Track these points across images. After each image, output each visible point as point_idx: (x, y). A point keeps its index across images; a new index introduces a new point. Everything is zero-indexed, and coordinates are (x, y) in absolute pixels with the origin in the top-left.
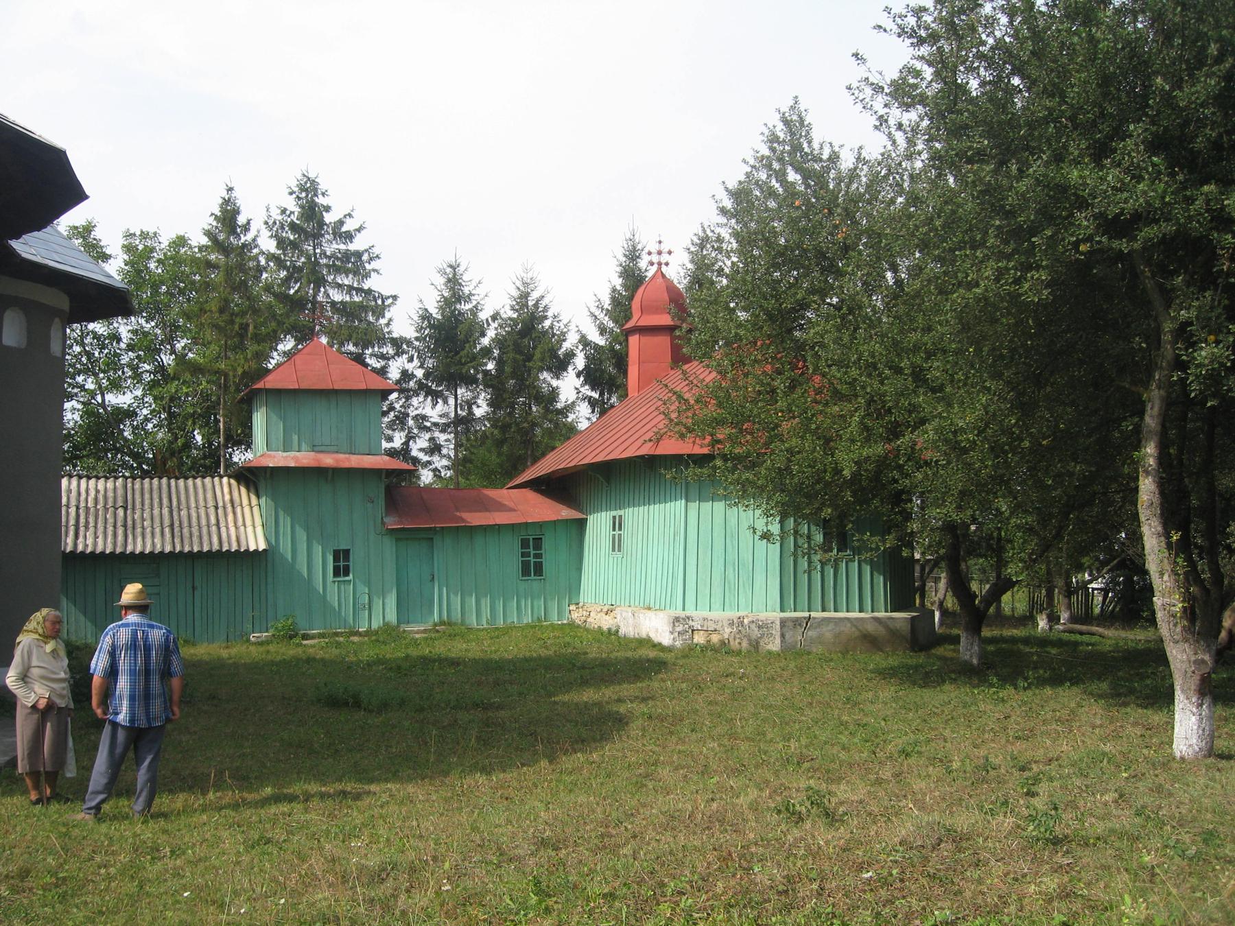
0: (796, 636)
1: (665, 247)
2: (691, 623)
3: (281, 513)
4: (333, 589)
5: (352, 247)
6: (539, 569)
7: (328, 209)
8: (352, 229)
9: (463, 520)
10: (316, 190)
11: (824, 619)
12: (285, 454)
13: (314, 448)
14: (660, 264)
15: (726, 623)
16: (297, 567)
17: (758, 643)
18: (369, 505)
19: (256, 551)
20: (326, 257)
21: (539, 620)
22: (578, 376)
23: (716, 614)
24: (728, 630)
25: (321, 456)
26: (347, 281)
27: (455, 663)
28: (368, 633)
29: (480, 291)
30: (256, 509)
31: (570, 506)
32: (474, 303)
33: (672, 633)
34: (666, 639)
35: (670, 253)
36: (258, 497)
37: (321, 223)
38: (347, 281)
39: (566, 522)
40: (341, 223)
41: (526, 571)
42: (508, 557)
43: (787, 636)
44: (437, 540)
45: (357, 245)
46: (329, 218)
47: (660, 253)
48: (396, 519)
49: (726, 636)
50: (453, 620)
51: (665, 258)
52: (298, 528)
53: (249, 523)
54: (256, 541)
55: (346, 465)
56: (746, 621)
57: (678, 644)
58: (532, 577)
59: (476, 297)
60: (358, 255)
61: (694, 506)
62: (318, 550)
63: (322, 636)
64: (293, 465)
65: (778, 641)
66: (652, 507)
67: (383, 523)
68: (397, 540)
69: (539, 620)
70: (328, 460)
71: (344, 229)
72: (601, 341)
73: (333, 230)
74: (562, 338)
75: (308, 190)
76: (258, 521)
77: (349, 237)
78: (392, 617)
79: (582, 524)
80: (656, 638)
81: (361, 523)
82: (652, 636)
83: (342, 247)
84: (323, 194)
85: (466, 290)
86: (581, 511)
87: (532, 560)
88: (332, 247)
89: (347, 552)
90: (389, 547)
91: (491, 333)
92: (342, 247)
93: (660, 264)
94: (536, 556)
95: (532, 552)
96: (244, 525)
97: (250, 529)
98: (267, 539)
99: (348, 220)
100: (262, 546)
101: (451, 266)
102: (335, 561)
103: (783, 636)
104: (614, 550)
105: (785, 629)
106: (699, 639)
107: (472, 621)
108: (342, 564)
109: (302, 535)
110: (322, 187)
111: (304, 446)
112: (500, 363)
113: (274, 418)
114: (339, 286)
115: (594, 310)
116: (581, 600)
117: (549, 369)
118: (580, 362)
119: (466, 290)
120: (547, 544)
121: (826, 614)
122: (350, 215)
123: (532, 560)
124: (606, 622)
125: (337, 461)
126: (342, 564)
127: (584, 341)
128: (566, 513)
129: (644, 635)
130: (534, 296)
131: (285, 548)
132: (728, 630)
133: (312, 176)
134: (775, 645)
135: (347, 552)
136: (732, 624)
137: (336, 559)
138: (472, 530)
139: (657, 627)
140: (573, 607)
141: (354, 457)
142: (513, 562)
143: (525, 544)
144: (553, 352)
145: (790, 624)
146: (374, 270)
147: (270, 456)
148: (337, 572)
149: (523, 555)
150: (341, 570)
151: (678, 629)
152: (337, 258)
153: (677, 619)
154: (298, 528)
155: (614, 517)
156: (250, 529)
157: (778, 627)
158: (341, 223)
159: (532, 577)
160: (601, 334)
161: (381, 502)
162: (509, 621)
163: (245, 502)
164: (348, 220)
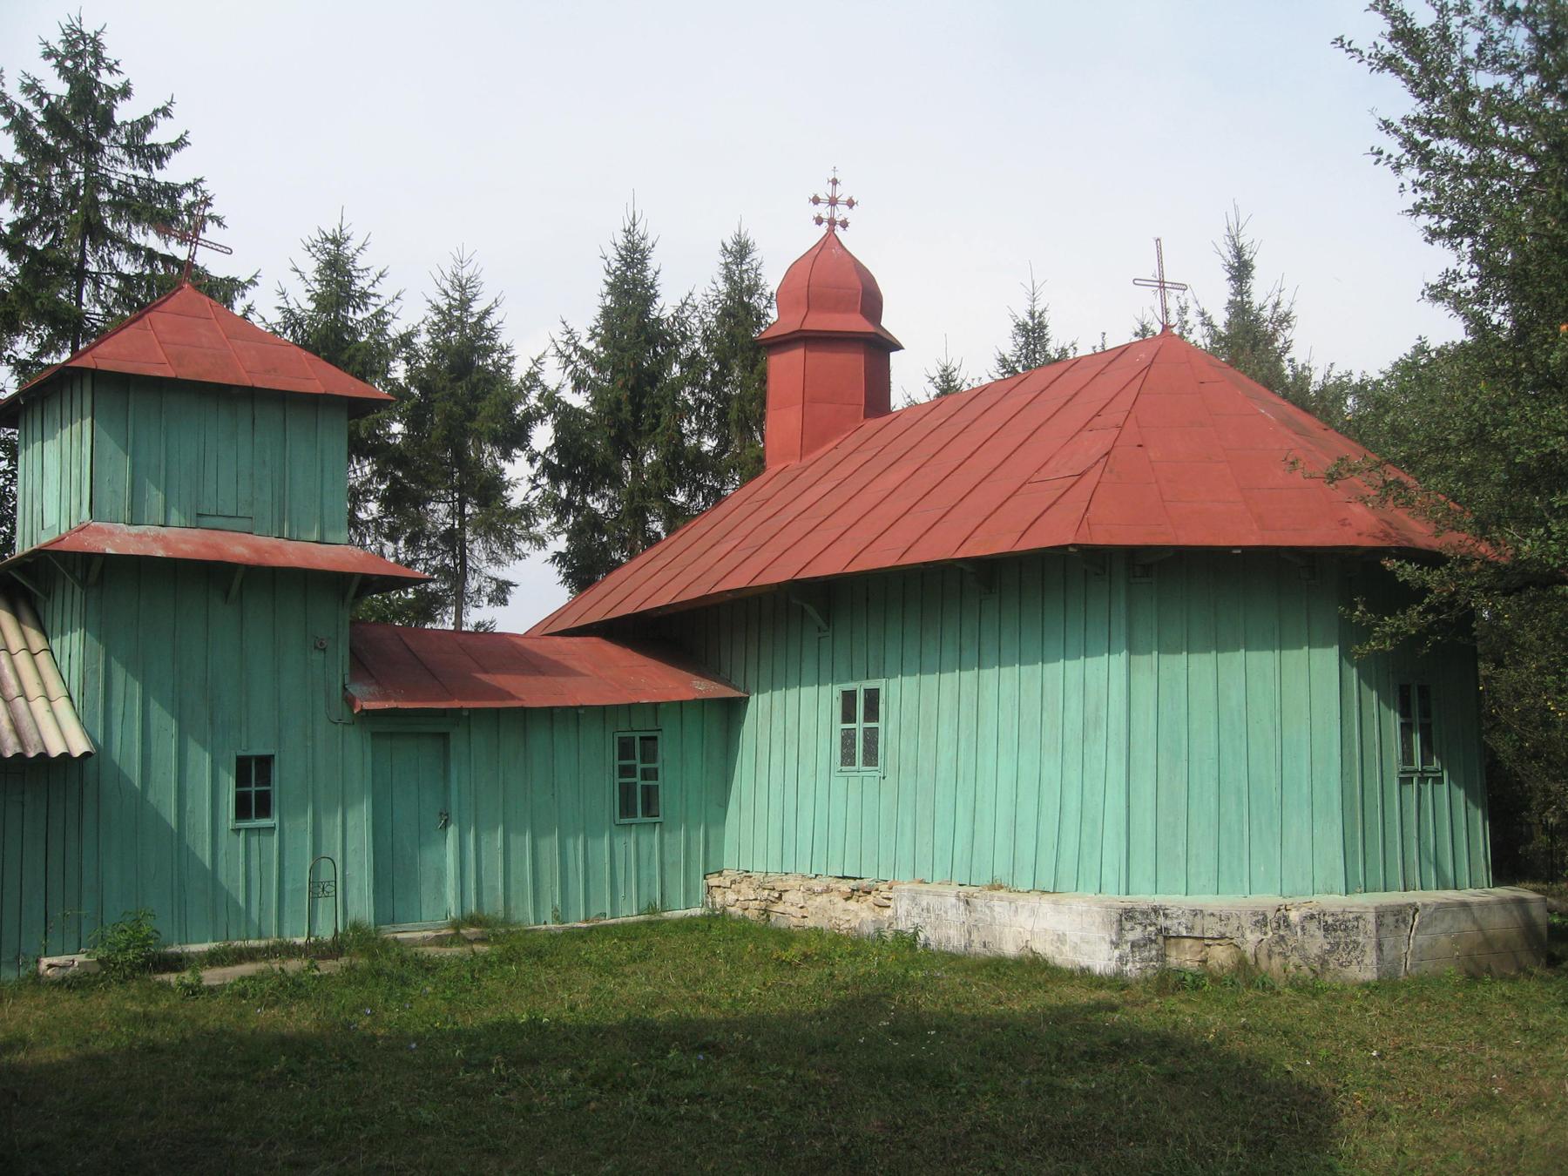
0: (1409, 946)
1: (843, 193)
2: (1161, 921)
3: (119, 674)
4: (234, 846)
5: (161, 176)
6: (650, 807)
7: (126, 92)
8: (162, 142)
9: (513, 697)
10: (97, 55)
11: (1443, 907)
12: (134, 530)
13: (198, 519)
14: (832, 222)
15: (1247, 922)
16: (151, 797)
17: (1324, 963)
18: (317, 657)
19: (66, 757)
20: (111, 190)
21: (651, 909)
22: (532, 460)
23: (1207, 900)
24: (1252, 937)
25: (217, 537)
26: (152, 241)
27: (696, 1039)
28: (316, 951)
29: (385, 290)
30: (44, 659)
31: (702, 674)
32: (373, 310)
33: (1116, 945)
34: (1100, 958)
35: (851, 204)
36: (43, 630)
37: (106, 122)
38: (152, 241)
39: (703, 704)
40: (147, 124)
41: (627, 809)
42: (592, 772)
43: (1386, 948)
44: (457, 743)
45: (172, 172)
46: (124, 113)
47: (833, 202)
48: (374, 689)
49: (1249, 949)
50: (487, 910)
51: (842, 212)
52: (155, 706)
53: (33, 689)
54: (62, 733)
55: (280, 561)
56: (1294, 916)
57: (1132, 969)
58: (640, 818)
59: (373, 300)
60: (172, 192)
61: (1146, 662)
62: (200, 761)
63: (214, 959)
64: (160, 553)
65: (1371, 957)
66: (989, 674)
67: (349, 701)
68: (375, 735)
69: (651, 909)
70: (238, 547)
71: (150, 139)
72: (579, 401)
73: (130, 136)
74: (520, 394)
75: (80, 55)
76: (56, 688)
77: (158, 155)
78: (362, 908)
79: (731, 711)
80: (1066, 957)
81: (292, 692)
82: (1044, 948)
83: (141, 173)
84: (110, 69)
85: (361, 284)
86: (728, 683)
87: (639, 781)
88: (122, 170)
89: (265, 762)
90: (356, 750)
91: (399, 371)
92: (141, 173)
93: (832, 222)
94: (646, 775)
95: (640, 766)
96: (24, 694)
97: (39, 706)
98: (89, 735)
99: (161, 121)
100: (79, 746)
101: (334, 241)
102: (237, 785)
103: (1380, 946)
104: (848, 758)
105: (1383, 931)
106: (1184, 958)
107: (525, 915)
108: (253, 789)
109: (165, 725)
110: (109, 54)
111: (175, 517)
112: (415, 421)
113: (110, 446)
114: (135, 250)
115: (562, 346)
116: (729, 862)
117: (495, 441)
118: (543, 436)
119: (361, 284)
120: (666, 750)
121: (1451, 895)
122: (165, 112)
123: (639, 781)
124: (858, 916)
125: (257, 549)
126: (253, 789)
127: (551, 400)
128: (703, 688)
129: (1010, 949)
130: (477, 307)
131: (127, 753)
132: (1252, 937)
133: (89, 30)
134: (1365, 969)
135: (265, 762)
136: (1261, 922)
137: (242, 779)
138: (526, 716)
139: (1070, 931)
140: (714, 881)
141: (290, 546)
142: (603, 787)
143: (626, 749)
144: (509, 406)
145: (1389, 920)
146: (212, 218)
147: (99, 531)
148: (242, 811)
149: (626, 771)
150: (253, 804)
151: (1130, 936)
152: (129, 195)
153: (1128, 915)
154: (155, 706)
155: (849, 698)
156: (39, 706)
157: (1371, 927)
158: (147, 124)
159: (640, 818)
160: (577, 389)
161: (343, 652)
162: (594, 912)
163: (15, 642)
164: (161, 121)
